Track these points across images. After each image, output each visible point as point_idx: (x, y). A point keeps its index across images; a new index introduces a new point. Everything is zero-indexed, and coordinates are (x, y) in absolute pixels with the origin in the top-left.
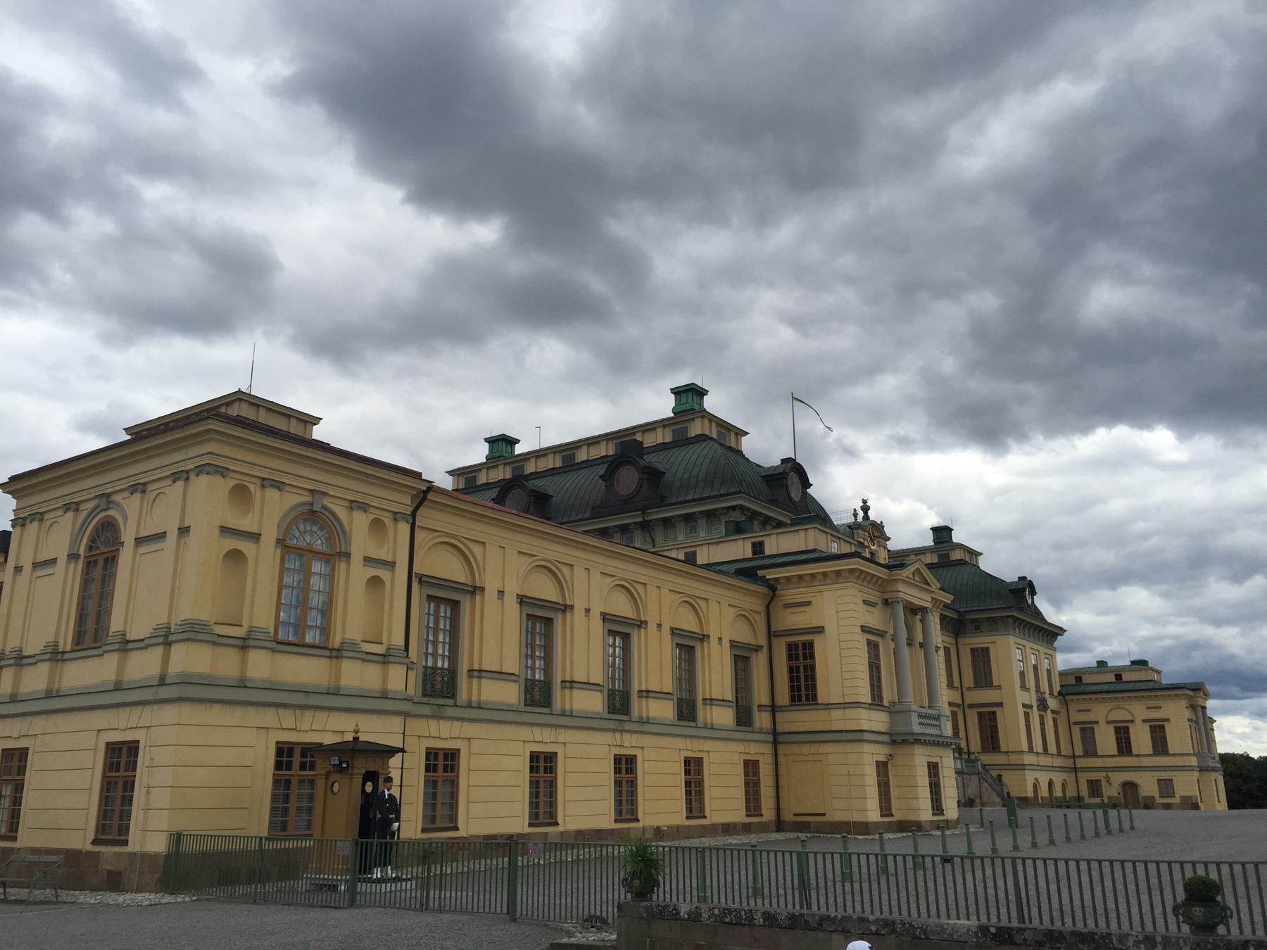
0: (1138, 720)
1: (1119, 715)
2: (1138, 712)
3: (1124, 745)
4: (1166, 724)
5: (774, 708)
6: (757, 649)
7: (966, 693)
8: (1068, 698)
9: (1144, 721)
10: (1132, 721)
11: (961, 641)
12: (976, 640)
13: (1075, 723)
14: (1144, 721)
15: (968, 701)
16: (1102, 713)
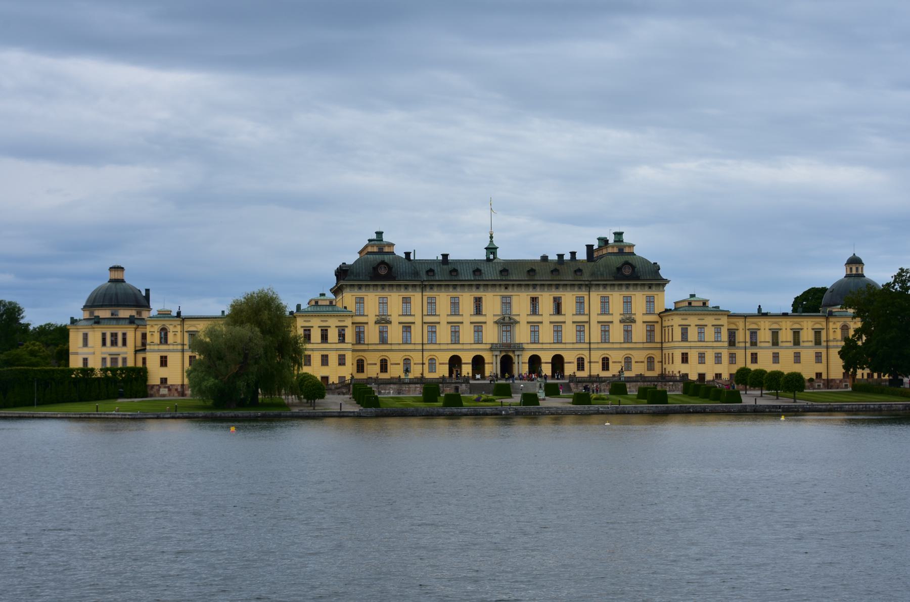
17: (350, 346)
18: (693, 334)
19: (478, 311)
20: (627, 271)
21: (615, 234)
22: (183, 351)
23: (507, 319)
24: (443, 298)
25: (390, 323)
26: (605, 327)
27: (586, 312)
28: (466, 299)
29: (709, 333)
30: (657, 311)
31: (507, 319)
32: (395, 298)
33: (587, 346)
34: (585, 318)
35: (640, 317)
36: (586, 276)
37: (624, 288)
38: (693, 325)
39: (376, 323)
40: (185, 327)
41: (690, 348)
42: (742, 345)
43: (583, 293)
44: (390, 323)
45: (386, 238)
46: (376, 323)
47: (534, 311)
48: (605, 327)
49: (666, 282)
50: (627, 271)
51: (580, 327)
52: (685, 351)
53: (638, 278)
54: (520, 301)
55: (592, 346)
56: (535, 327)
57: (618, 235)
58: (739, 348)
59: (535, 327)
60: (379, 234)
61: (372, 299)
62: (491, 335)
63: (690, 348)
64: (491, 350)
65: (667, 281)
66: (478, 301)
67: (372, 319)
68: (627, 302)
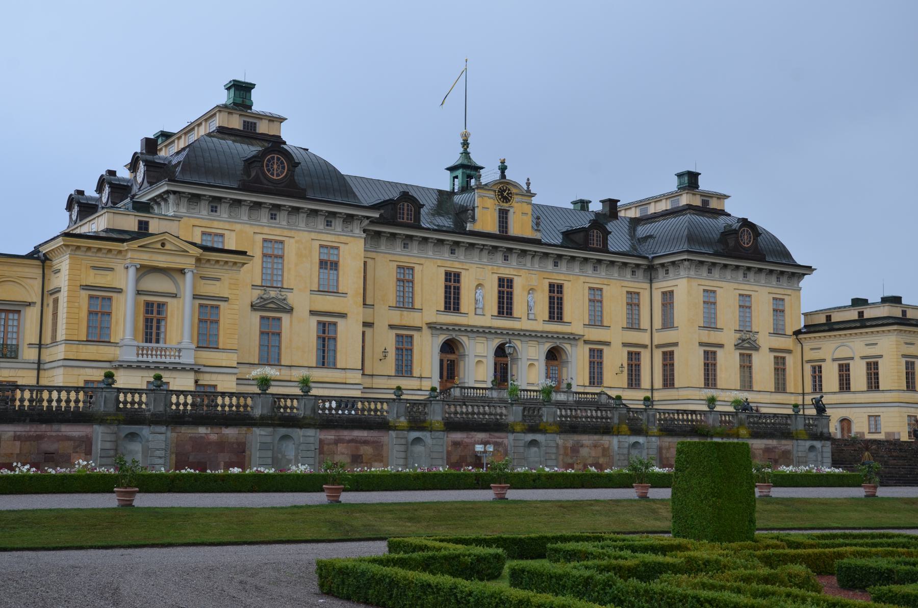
0: (857, 359)
1: (843, 353)
2: (856, 347)
3: (845, 384)
4: (880, 361)
5: (40, 346)
6: (30, 304)
7: (655, 335)
8: (801, 336)
9: (863, 358)
10: (852, 358)
11: (655, 285)
12: (665, 284)
13: (808, 361)
14: (863, 358)
15: (656, 342)
16: (829, 349)
17: (230, 359)
21: (680, 175)
25: (290, 310)
30: (789, 331)
35: (766, 341)
39: (254, 307)
44: (290, 310)
45: (260, 102)
46: (254, 307)
49: (809, 269)
50: (746, 241)
53: (762, 259)
57: (690, 180)
60: (241, 90)
65: (809, 269)
68: (745, 305)
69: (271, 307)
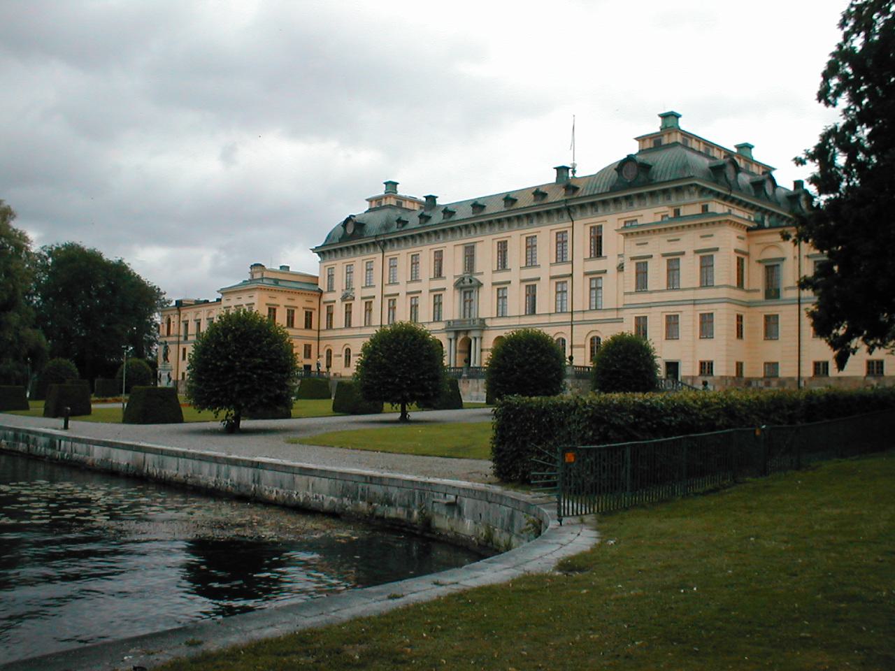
18: (657, 273)
19: (439, 274)
20: (630, 174)
22: (179, 343)
23: (467, 280)
24: (402, 255)
26: (595, 278)
27: (569, 259)
28: (426, 252)
29: (690, 269)
31: (467, 280)
32: (358, 261)
33: (567, 318)
34: (564, 269)
36: (579, 194)
37: (624, 205)
38: (656, 255)
40: (182, 315)
41: (649, 305)
42: (793, 294)
43: (563, 225)
47: (503, 265)
48: (595, 278)
51: (562, 283)
52: (641, 312)
53: (649, 182)
54: (486, 246)
55: (577, 317)
56: (501, 288)
57: (670, 118)
58: (788, 302)
59: (501, 288)
61: (339, 265)
62: (452, 308)
63: (649, 305)
64: (447, 330)
66: (439, 257)
67: (336, 296)
69: (347, 298)
